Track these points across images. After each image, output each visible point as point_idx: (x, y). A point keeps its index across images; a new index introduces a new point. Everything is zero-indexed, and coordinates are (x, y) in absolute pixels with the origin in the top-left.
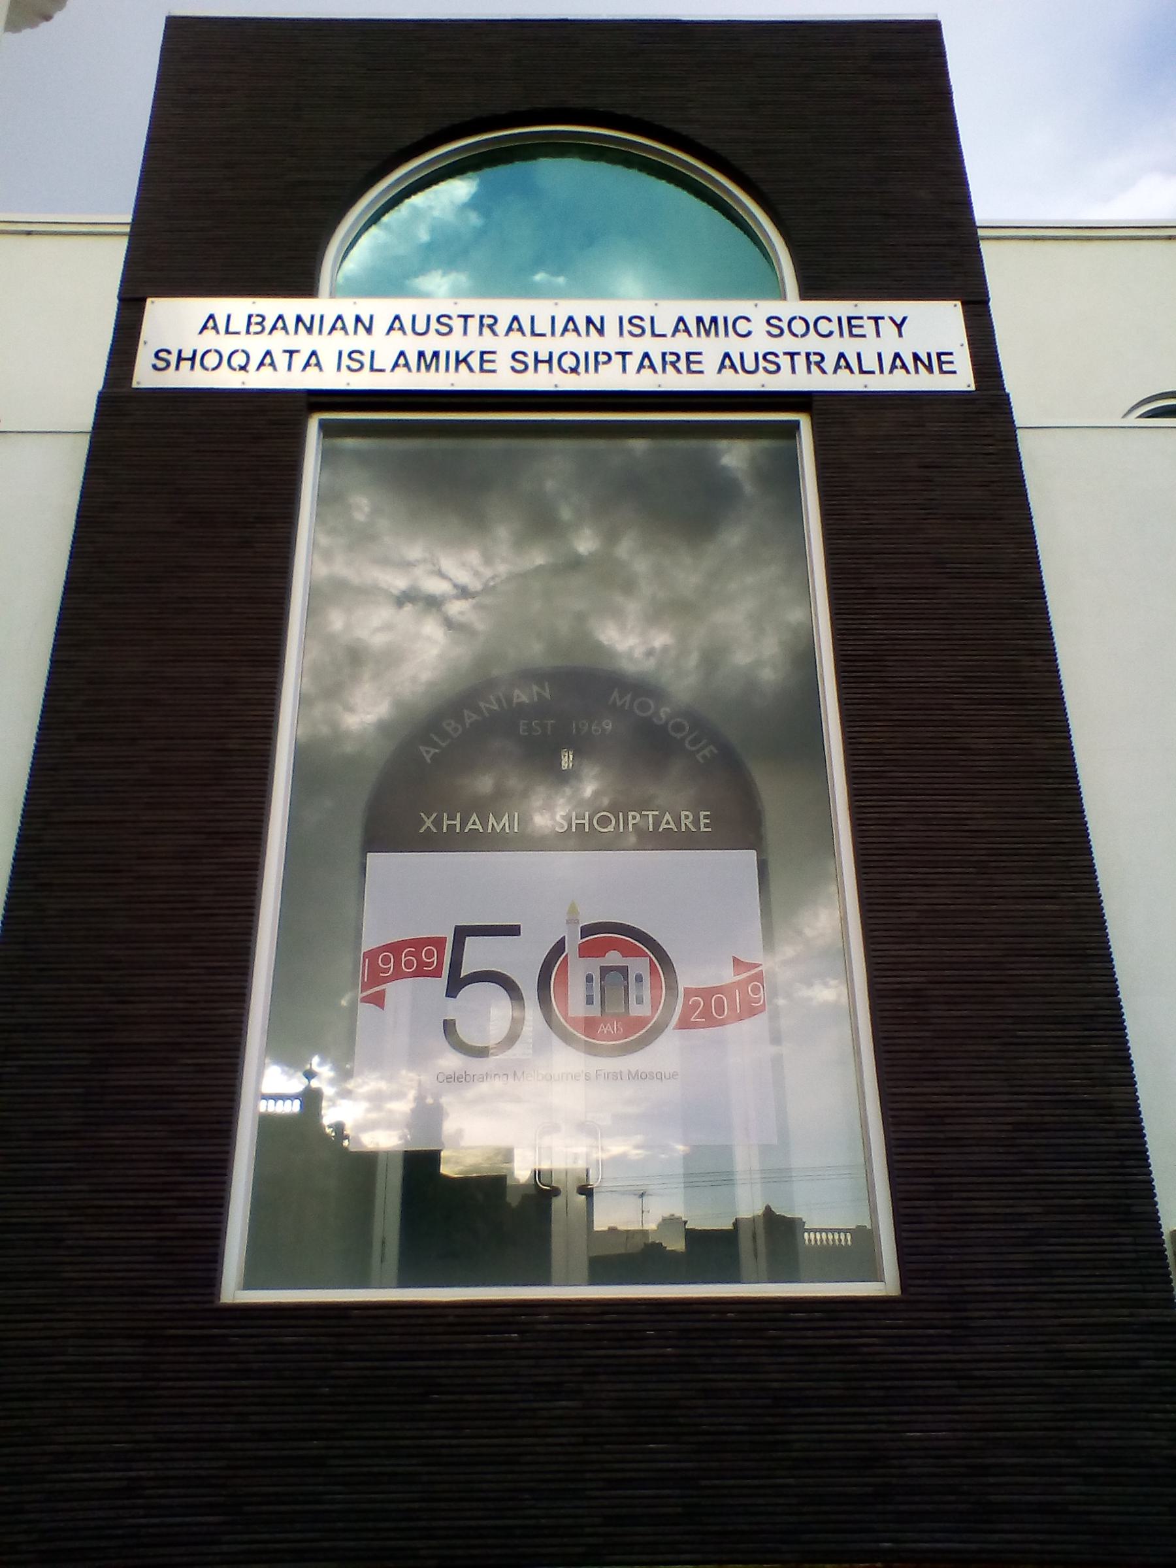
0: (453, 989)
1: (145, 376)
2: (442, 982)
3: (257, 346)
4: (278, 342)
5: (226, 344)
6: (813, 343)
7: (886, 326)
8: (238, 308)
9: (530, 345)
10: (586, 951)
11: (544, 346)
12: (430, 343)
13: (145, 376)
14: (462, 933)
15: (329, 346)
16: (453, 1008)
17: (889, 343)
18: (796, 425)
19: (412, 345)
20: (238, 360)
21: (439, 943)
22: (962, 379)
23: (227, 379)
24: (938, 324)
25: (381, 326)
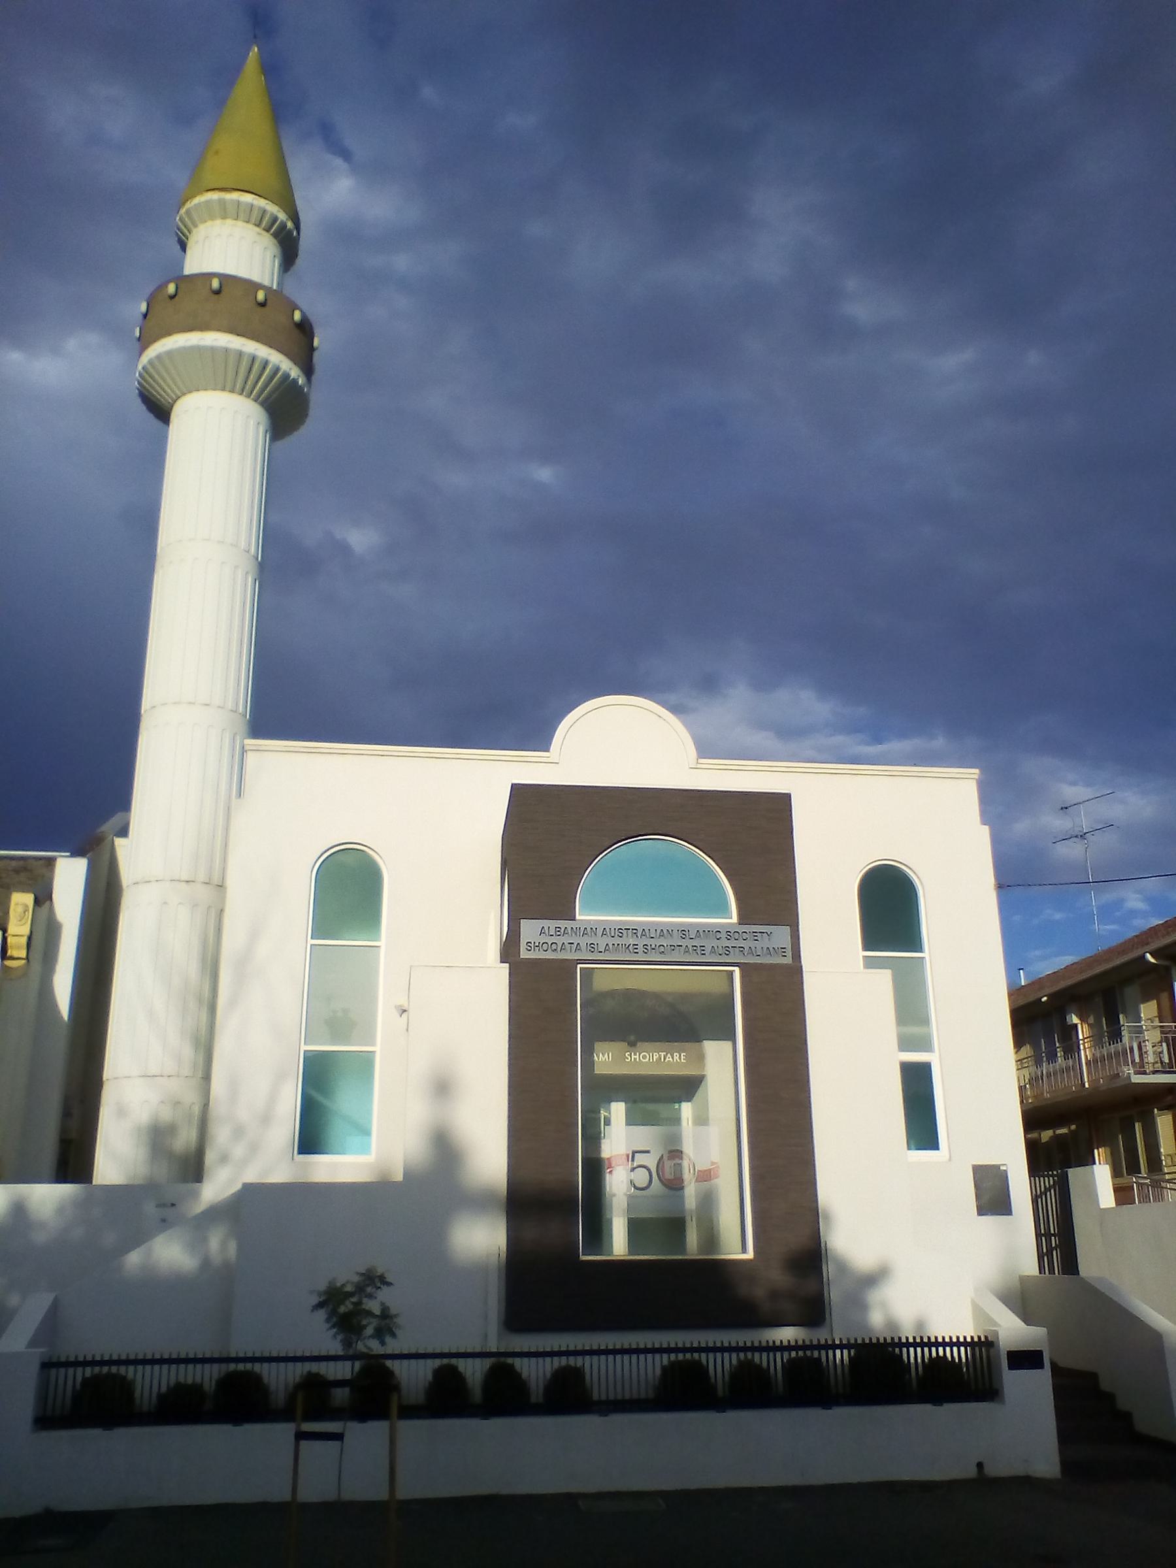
0: (633, 1169)
1: (524, 954)
3: (559, 940)
4: (566, 940)
6: (741, 943)
9: (649, 942)
10: (670, 1158)
11: (653, 942)
12: (617, 941)
13: (524, 954)
14: (634, 1153)
15: (584, 941)
16: (632, 1175)
17: (764, 942)
18: (731, 973)
19: (611, 941)
20: (554, 946)
22: (788, 960)
23: (550, 955)
24: (781, 935)
25: (600, 932)
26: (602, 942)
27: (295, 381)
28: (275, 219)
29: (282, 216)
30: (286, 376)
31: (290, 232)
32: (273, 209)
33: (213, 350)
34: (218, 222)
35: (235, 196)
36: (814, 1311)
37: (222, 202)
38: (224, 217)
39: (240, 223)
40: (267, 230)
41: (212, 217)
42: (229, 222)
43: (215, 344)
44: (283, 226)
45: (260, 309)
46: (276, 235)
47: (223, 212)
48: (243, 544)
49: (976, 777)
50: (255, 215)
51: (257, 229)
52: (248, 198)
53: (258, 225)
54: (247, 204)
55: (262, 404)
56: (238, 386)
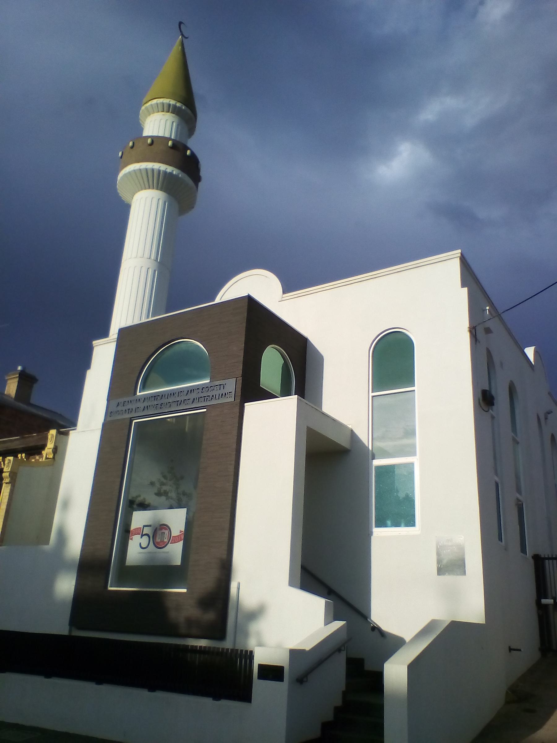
2: (140, 536)
5: (120, 408)
7: (222, 386)
8: (121, 400)
14: (144, 526)
21: (140, 528)
26: (141, 405)
27: (171, 174)
28: (169, 105)
29: (173, 102)
30: (165, 172)
31: (180, 108)
32: (166, 101)
33: (129, 173)
34: (148, 118)
35: (150, 103)
36: (218, 630)
37: (146, 108)
38: (150, 115)
39: (156, 114)
40: (168, 112)
41: (146, 117)
42: (152, 115)
43: (130, 170)
44: (175, 106)
45: (152, 146)
46: (173, 112)
47: (149, 112)
48: (147, 255)
49: (459, 255)
50: (160, 108)
51: (163, 113)
52: (155, 101)
53: (163, 111)
54: (155, 104)
55: (161, 190)
56: (151, 186)
